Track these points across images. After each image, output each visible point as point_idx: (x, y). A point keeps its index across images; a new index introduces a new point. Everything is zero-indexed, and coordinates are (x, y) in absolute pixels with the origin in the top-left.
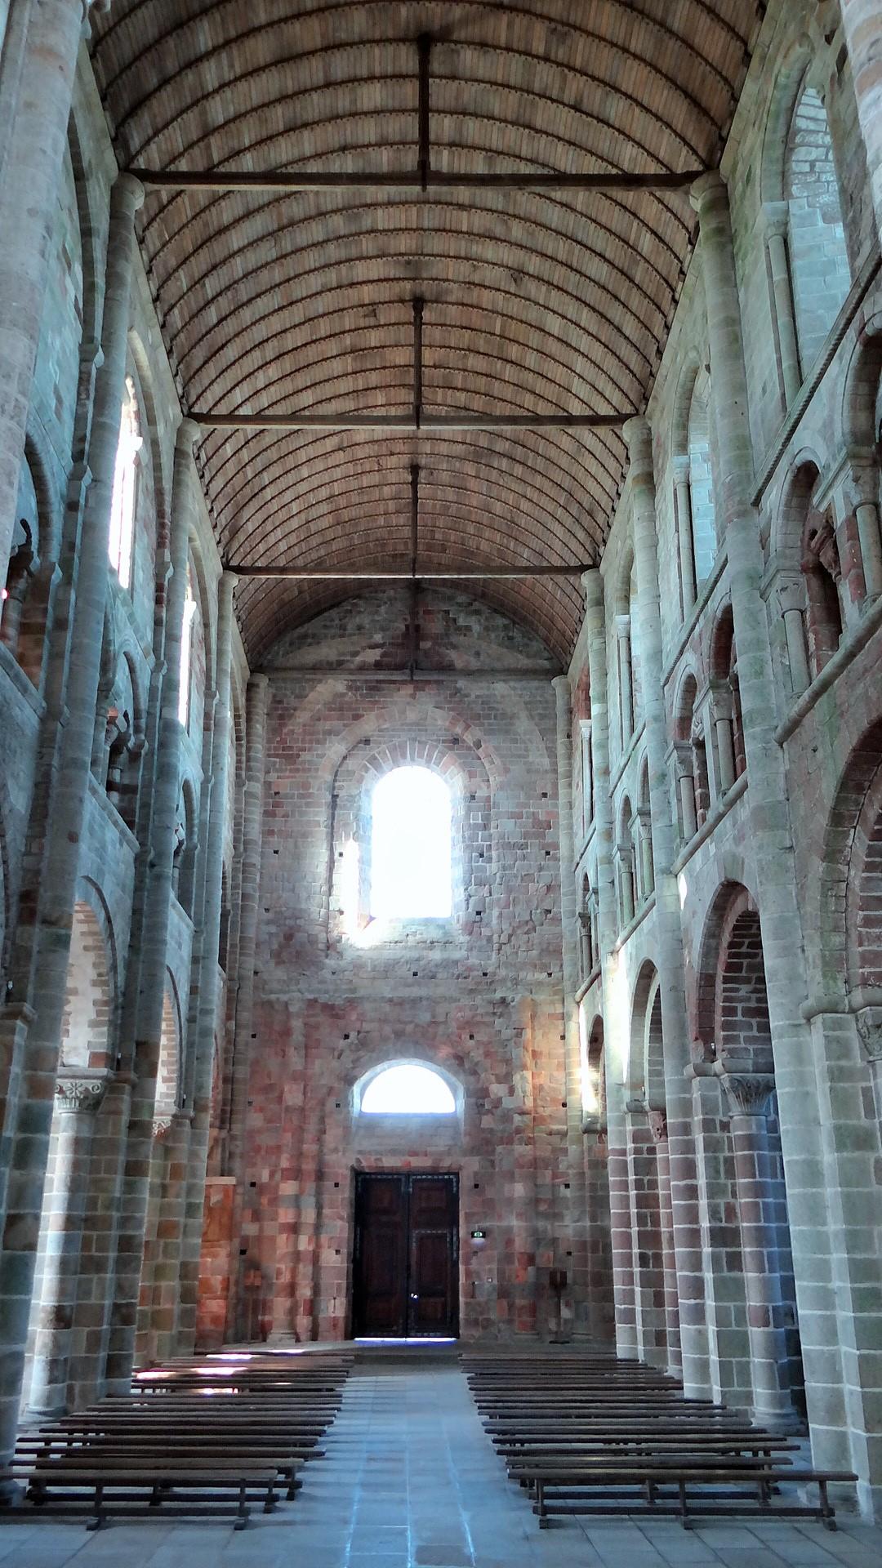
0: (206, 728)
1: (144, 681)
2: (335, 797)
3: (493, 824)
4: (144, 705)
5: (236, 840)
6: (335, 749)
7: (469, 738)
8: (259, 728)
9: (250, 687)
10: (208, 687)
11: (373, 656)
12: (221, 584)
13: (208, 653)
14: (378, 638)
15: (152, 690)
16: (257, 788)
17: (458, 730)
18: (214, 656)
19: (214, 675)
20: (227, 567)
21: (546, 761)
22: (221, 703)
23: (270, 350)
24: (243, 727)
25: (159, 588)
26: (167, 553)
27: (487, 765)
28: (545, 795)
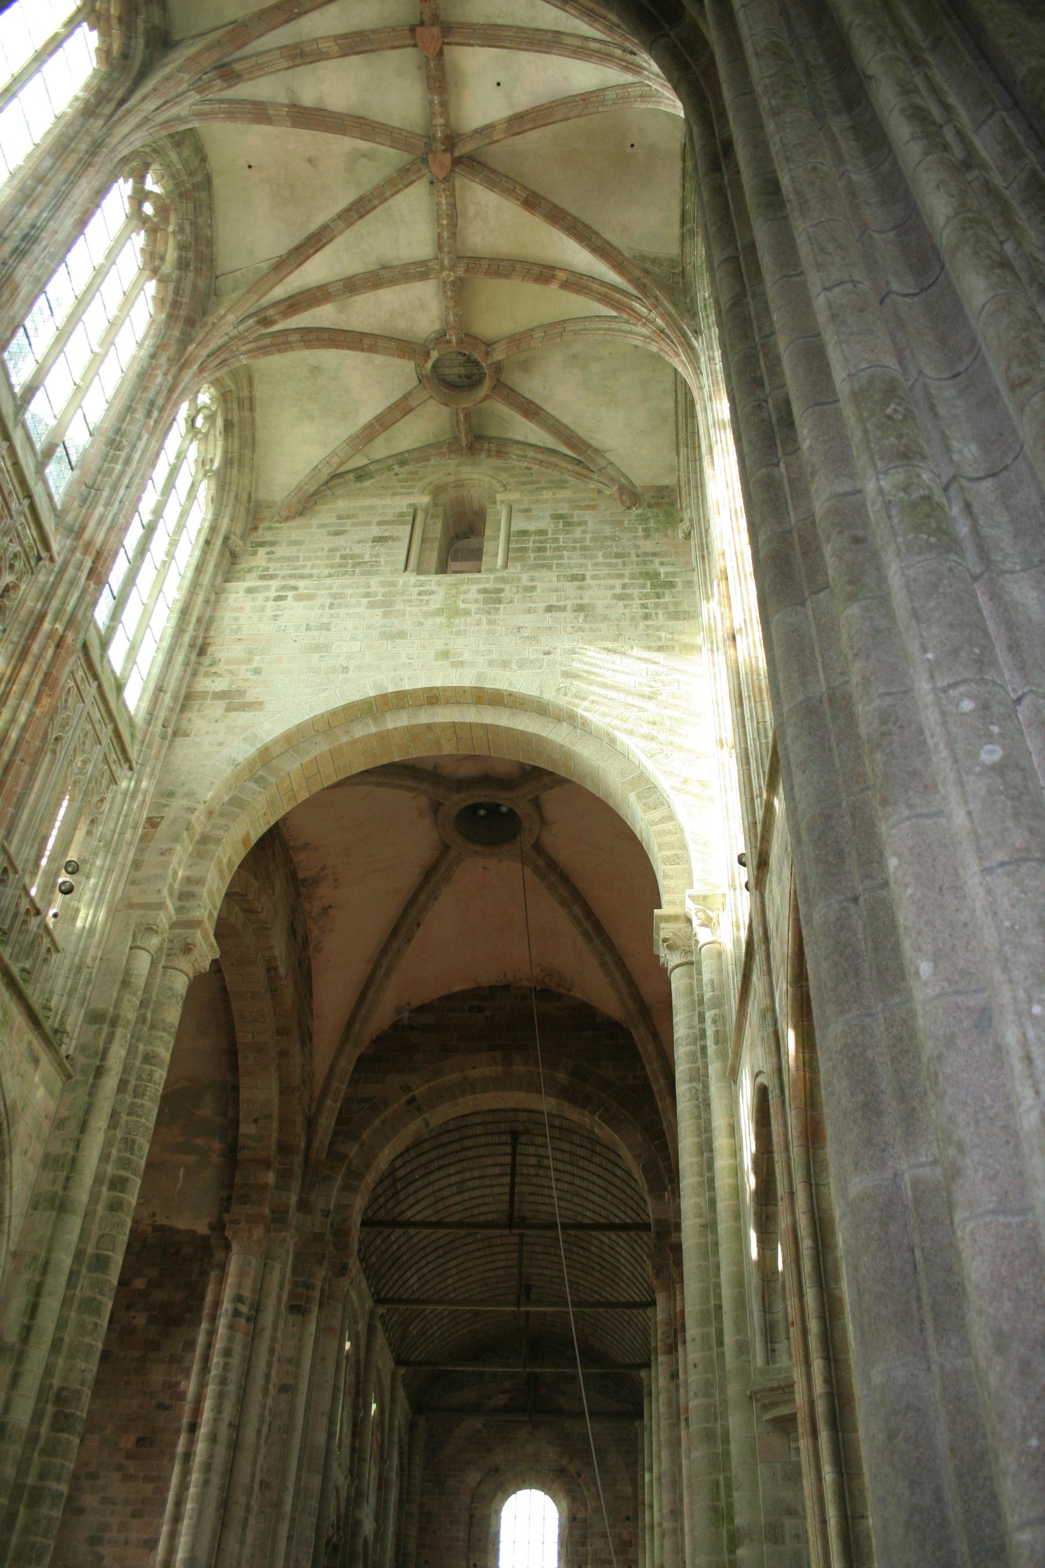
0: (379, 1488)
1: (344, 1494)
2: (472, 1516)
3: (589, 1541)
4: (342, 1512)
5: (397, 1553)
6: (473, 1477)
7: (572, 1469)
8: (418, 1459)
9: (412, 1426)
10: (382, 1458)
11: (502, 1400)
12: (394, 1375)
13: (383, 1432)
14: (507, 1384)
15: (348, 1498)
16: (414, 1508)
17: (564, 1462)
18: (387, 1415)
19: (386, 1445)
20: (399, 1362)
21: (629, 1489)
22: (390, 1468)
23: (428, 1250)
24: (405, 1461)
25: (355, 1425)
26: (361, 1400)
27: (586, 1493)
28: (628, 1518)
